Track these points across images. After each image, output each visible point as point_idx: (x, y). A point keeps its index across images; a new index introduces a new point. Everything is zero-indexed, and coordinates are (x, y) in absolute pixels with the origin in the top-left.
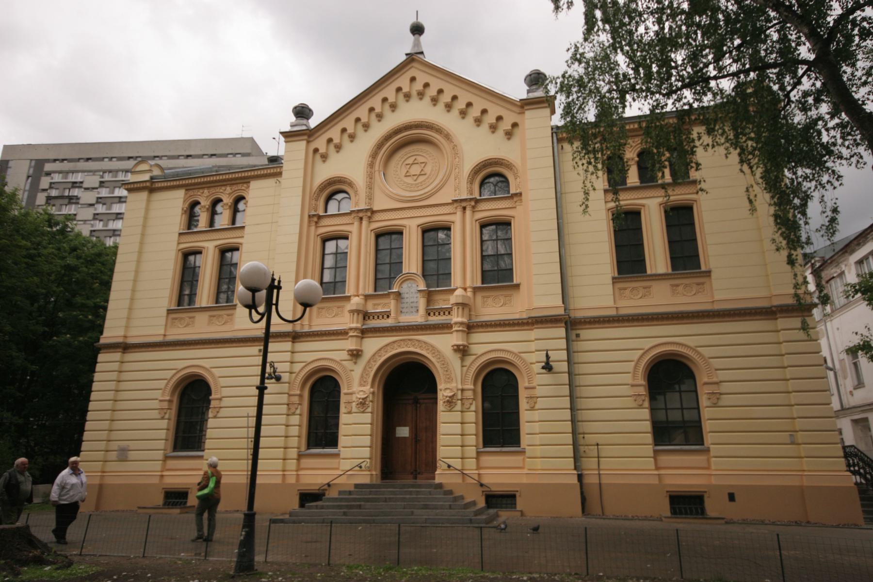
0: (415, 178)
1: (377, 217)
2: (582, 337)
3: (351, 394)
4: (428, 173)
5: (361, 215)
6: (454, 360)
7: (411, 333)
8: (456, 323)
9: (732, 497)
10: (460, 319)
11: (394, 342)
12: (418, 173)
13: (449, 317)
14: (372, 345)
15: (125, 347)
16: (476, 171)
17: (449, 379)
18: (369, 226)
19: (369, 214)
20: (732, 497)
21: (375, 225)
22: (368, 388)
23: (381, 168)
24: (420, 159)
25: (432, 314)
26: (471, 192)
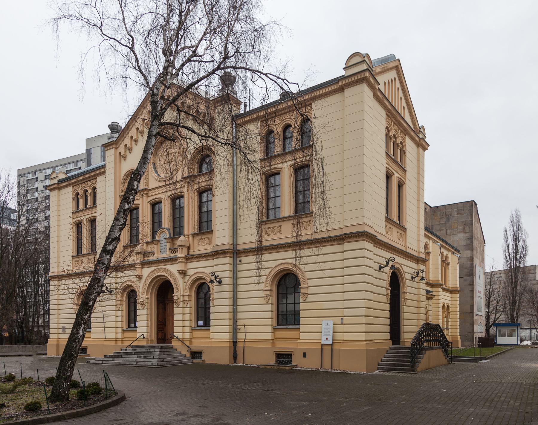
1: (151, 193)
2: (243, 262)
7: (163, 264)
9: (305, 355)
11: (155, 270)
13: (176, 254)
14: (146, 272)
15: (59, 277)
19: (146, 192)
20: (305, 355)
21: (150, 199)
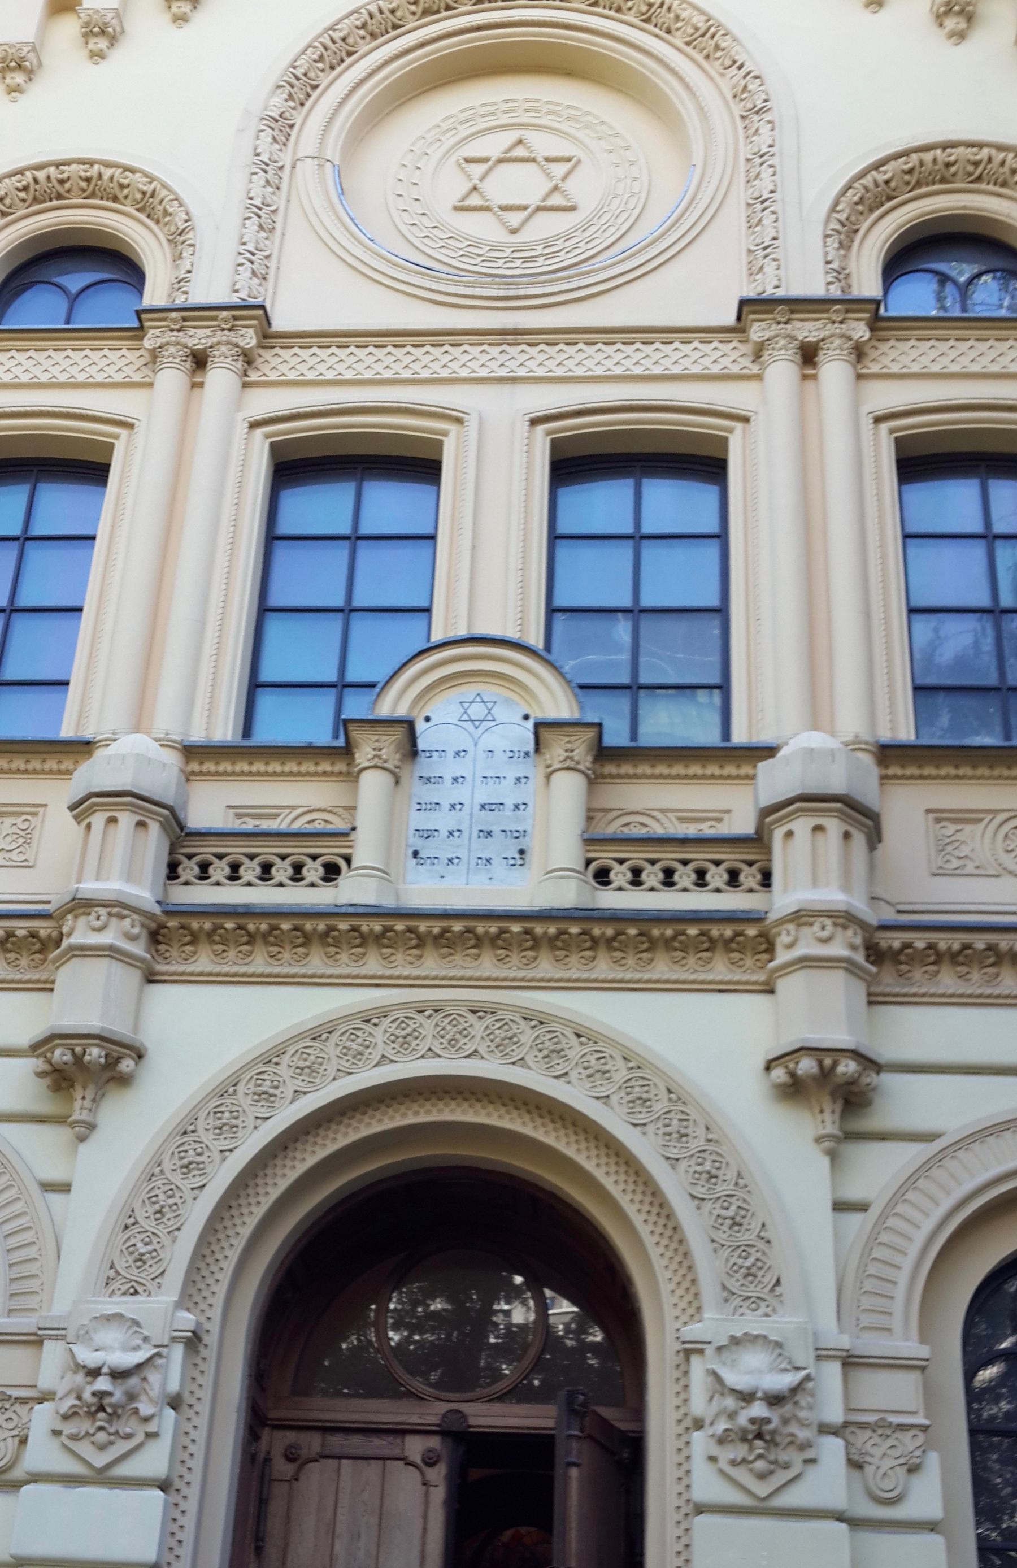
0: (514, 219)
3: (35, 1341)
4: (587, 207)
5: (199, 337)
6: (784, 1153)
8: (800, 917)
10: (832, 895)
11: (369, 1018)
12: (533, 200)
16: (874, 191)
17: (755, 1276)
18: (238, 405)
22: (160, 1308)
23: (333, 151)
24: (543, 144)
25: (620, 875)
26: (842, 275)
